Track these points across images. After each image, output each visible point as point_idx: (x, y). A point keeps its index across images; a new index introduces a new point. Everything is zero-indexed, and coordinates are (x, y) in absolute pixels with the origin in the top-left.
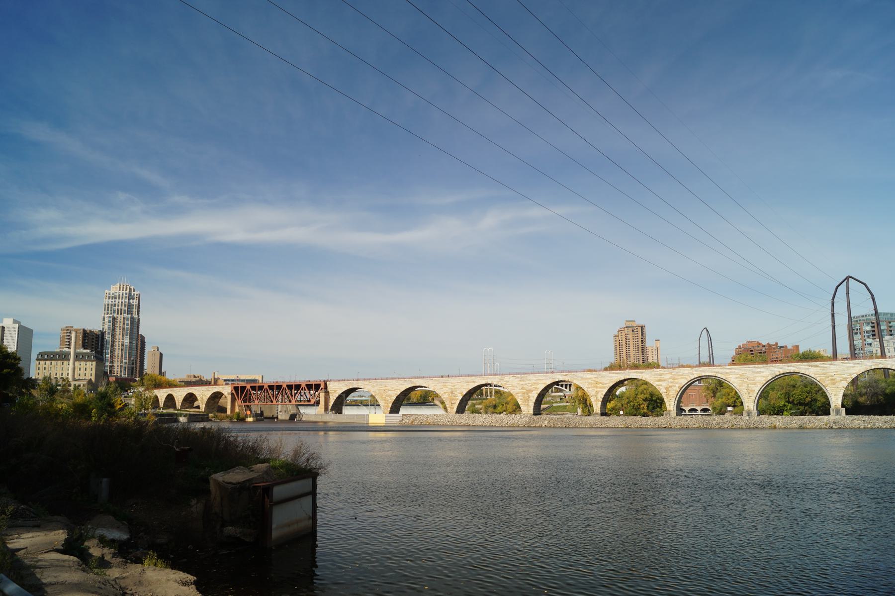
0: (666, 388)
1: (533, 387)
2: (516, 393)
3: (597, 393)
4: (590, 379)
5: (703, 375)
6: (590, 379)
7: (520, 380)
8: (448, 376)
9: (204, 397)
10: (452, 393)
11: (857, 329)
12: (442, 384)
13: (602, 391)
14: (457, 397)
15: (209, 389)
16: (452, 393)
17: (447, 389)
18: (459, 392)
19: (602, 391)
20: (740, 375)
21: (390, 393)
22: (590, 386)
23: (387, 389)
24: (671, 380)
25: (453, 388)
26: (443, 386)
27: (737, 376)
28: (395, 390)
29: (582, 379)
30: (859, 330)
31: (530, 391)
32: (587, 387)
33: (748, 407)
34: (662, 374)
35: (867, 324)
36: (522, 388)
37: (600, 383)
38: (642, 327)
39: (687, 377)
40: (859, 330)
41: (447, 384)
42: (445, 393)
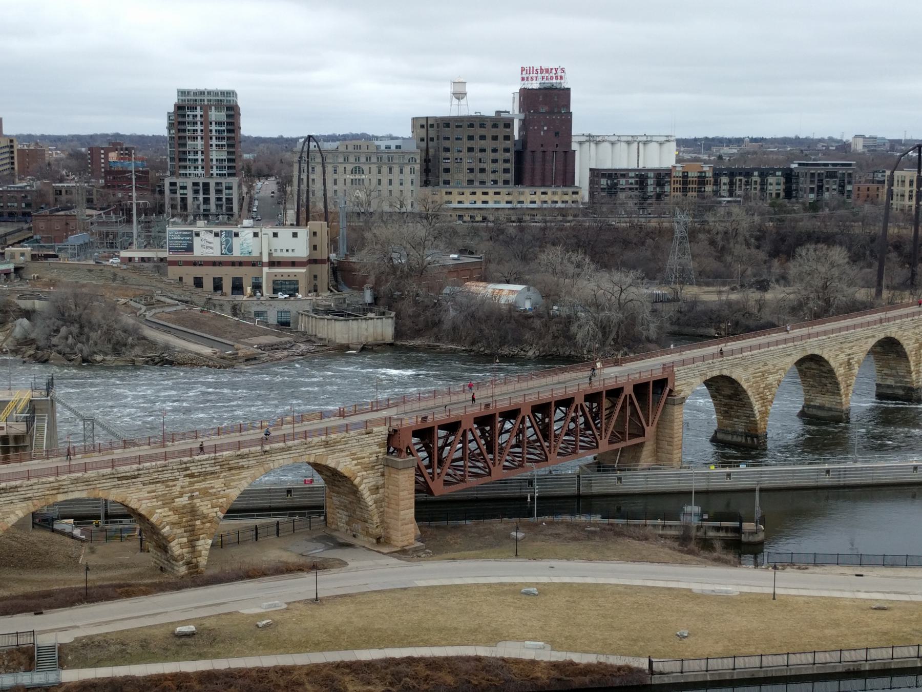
14: (853, 371)
16: (849, 363)
25: (850, 352)
35: (218, 108)
41: (843, 345)
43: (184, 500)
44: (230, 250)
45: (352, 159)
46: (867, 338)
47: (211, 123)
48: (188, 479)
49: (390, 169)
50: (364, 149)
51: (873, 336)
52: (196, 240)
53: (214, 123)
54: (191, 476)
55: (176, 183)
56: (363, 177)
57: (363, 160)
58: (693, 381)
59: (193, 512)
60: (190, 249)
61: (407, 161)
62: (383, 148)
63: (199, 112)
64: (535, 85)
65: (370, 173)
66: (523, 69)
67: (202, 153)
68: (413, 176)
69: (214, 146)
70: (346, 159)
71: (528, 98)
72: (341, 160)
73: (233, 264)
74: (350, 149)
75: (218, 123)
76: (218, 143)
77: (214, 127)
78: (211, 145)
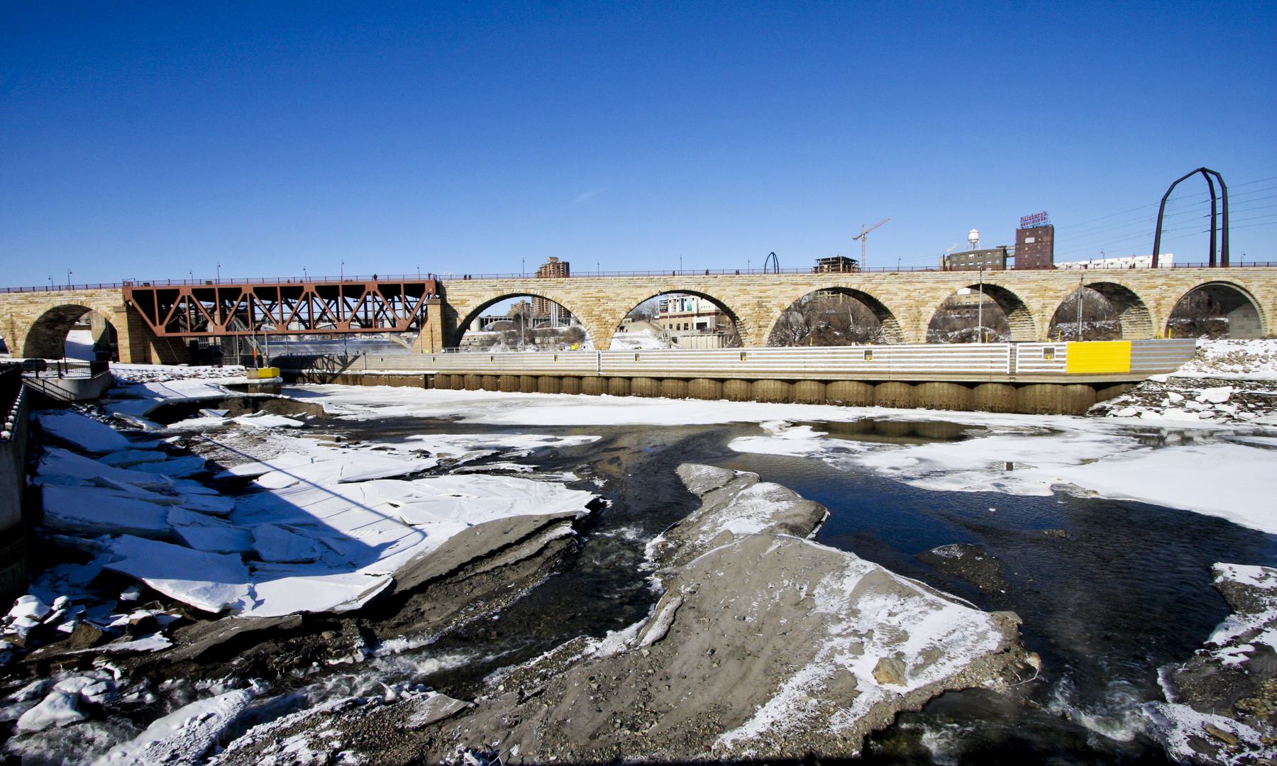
0: (1156, 300)
1: (928, 295)
2: (896, 307)
3: (1044, 306)
4: (1035, 281)
5: (1214, 279)
6: (1035, 282)
7: (905, 282)
8: (707, 273)
9: (19, 322)
10: (760, 305)
12: (739, 287)
13: (1053, 304)
14: (771, 314)
15: (37, 299)
16: (760, 305)
17: (749, 297)
18: (776, 302)
19: (1053, 304)
20: (1267, 282)
21: (611, 305)
22: (1033, 295)
23: (603, 298)
24: (1165, 287)
26: (740, 290)
27: (1262, 283)
28: (624, 300)
29: (1020, 281)
31: (925, 303)
32: (1027, 297)
33: (1271, 330)
34: (1153, 277)
36: (908, 297)
37: (1051, 290)
38: (568, 264)
39: (1189, 283)
41: (748, 288)
42: (744, 305)
43: (8, 317)
44: (683, 309)
46: (797, 284)
48: (9, 306)
51: (810, 284)
52: (670, 306)
54: (10, 303)
58: (483, 293)
59: (12, 323)
60: (667, 310)
64: (1030, 226)
66: (1022, 219)
71: (1021, 234)
73: (684, 316)
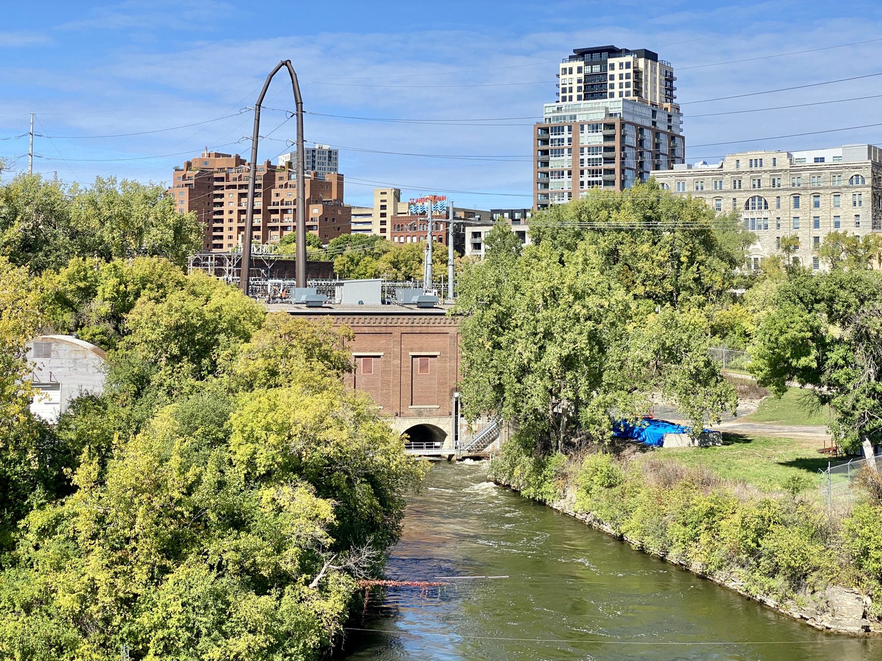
11: (563, 140)
30: (566, 143)
35: (595, 127)
40: (566, 143)
45: (746, 183)
47: (582, 149)
49: (797, 198)
50: (768, 165)
53: (586, 150)
55: (480, 233)
56: (765, 214)
57: (766, 183)
61: (847, 183)
62: (810, 161)
63: (566, 135)
65: (779, 206)
67: (570, 195)
68: (858, 210)
69: (586, 184)
70: (737, 184)
72: (727, 185)
74: (744, 166)
75: (592, 150)
76: (591, 179)
77: (586, 157)
78: (582, 183)
